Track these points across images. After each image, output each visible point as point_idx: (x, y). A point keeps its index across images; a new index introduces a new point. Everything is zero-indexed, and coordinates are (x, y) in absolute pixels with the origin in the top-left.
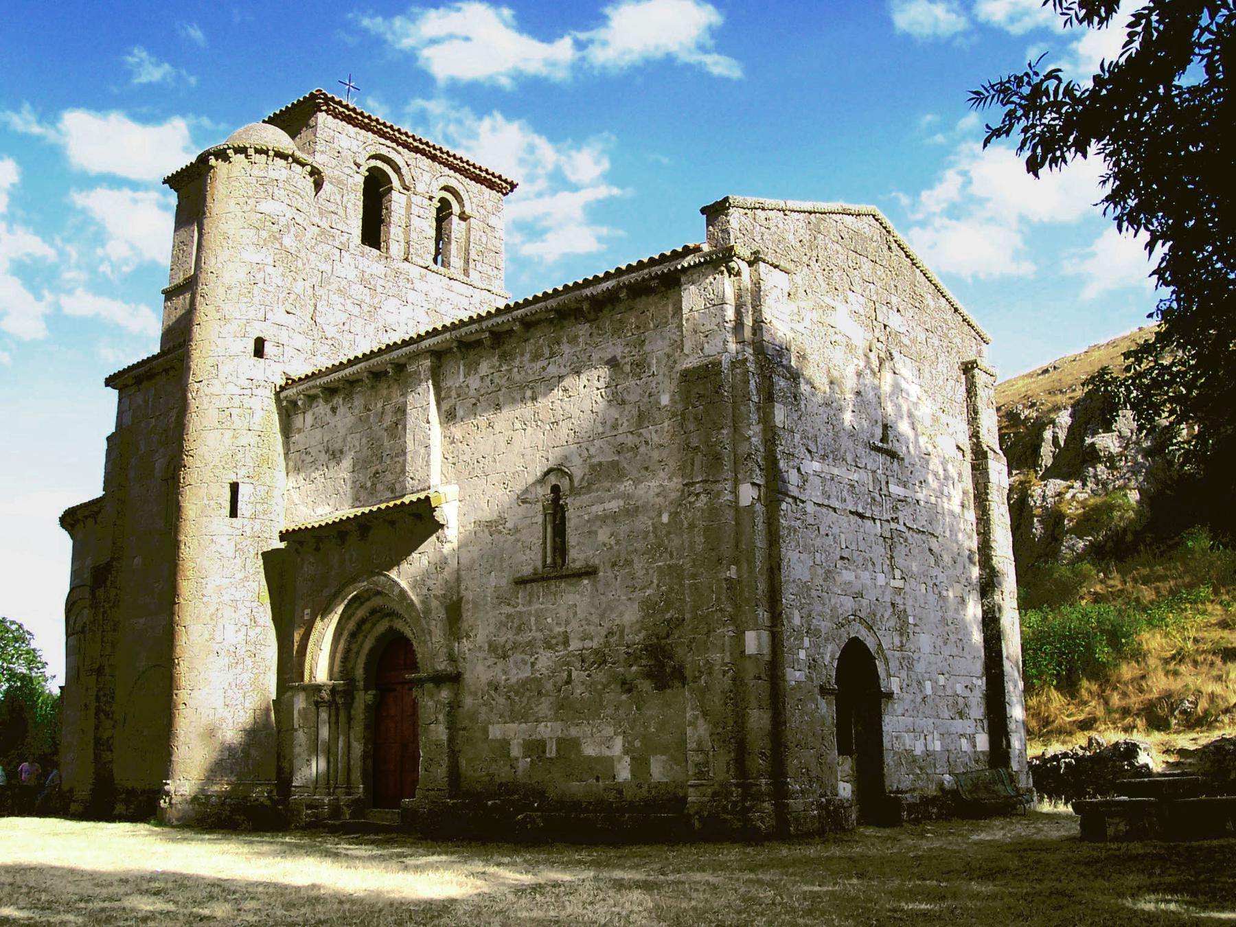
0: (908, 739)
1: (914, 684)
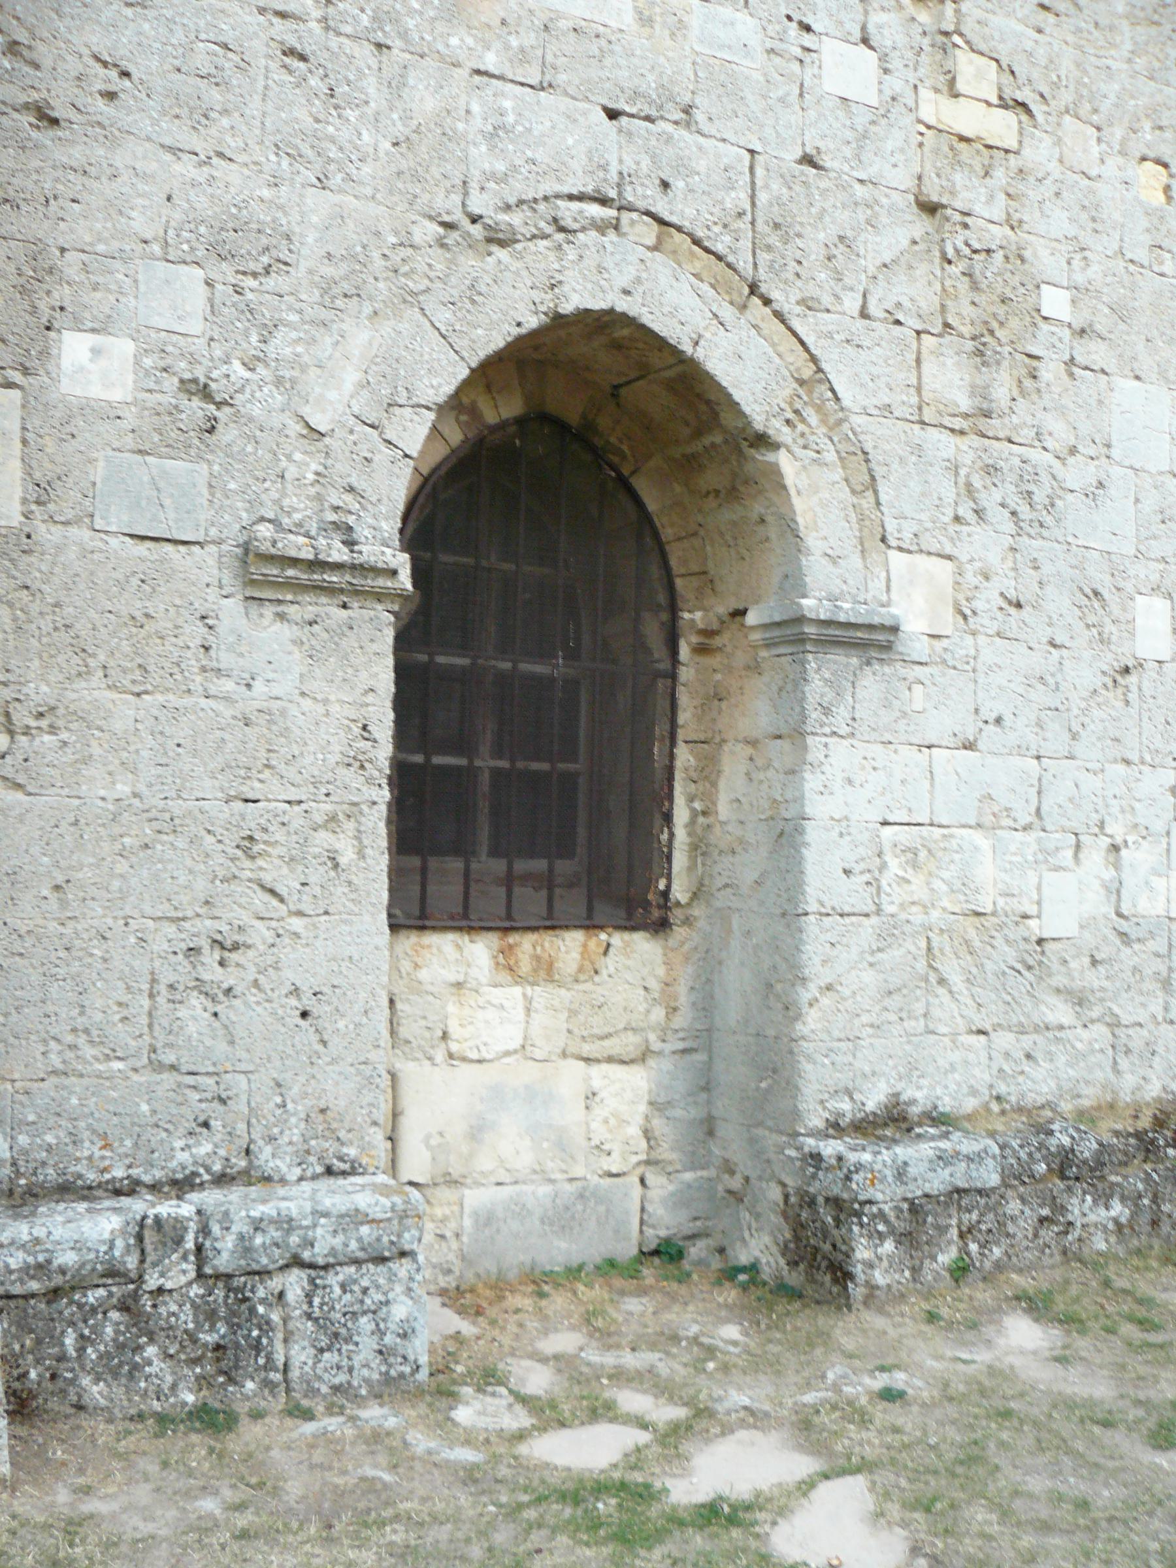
0: (989, 868)
1: (1059, 602)
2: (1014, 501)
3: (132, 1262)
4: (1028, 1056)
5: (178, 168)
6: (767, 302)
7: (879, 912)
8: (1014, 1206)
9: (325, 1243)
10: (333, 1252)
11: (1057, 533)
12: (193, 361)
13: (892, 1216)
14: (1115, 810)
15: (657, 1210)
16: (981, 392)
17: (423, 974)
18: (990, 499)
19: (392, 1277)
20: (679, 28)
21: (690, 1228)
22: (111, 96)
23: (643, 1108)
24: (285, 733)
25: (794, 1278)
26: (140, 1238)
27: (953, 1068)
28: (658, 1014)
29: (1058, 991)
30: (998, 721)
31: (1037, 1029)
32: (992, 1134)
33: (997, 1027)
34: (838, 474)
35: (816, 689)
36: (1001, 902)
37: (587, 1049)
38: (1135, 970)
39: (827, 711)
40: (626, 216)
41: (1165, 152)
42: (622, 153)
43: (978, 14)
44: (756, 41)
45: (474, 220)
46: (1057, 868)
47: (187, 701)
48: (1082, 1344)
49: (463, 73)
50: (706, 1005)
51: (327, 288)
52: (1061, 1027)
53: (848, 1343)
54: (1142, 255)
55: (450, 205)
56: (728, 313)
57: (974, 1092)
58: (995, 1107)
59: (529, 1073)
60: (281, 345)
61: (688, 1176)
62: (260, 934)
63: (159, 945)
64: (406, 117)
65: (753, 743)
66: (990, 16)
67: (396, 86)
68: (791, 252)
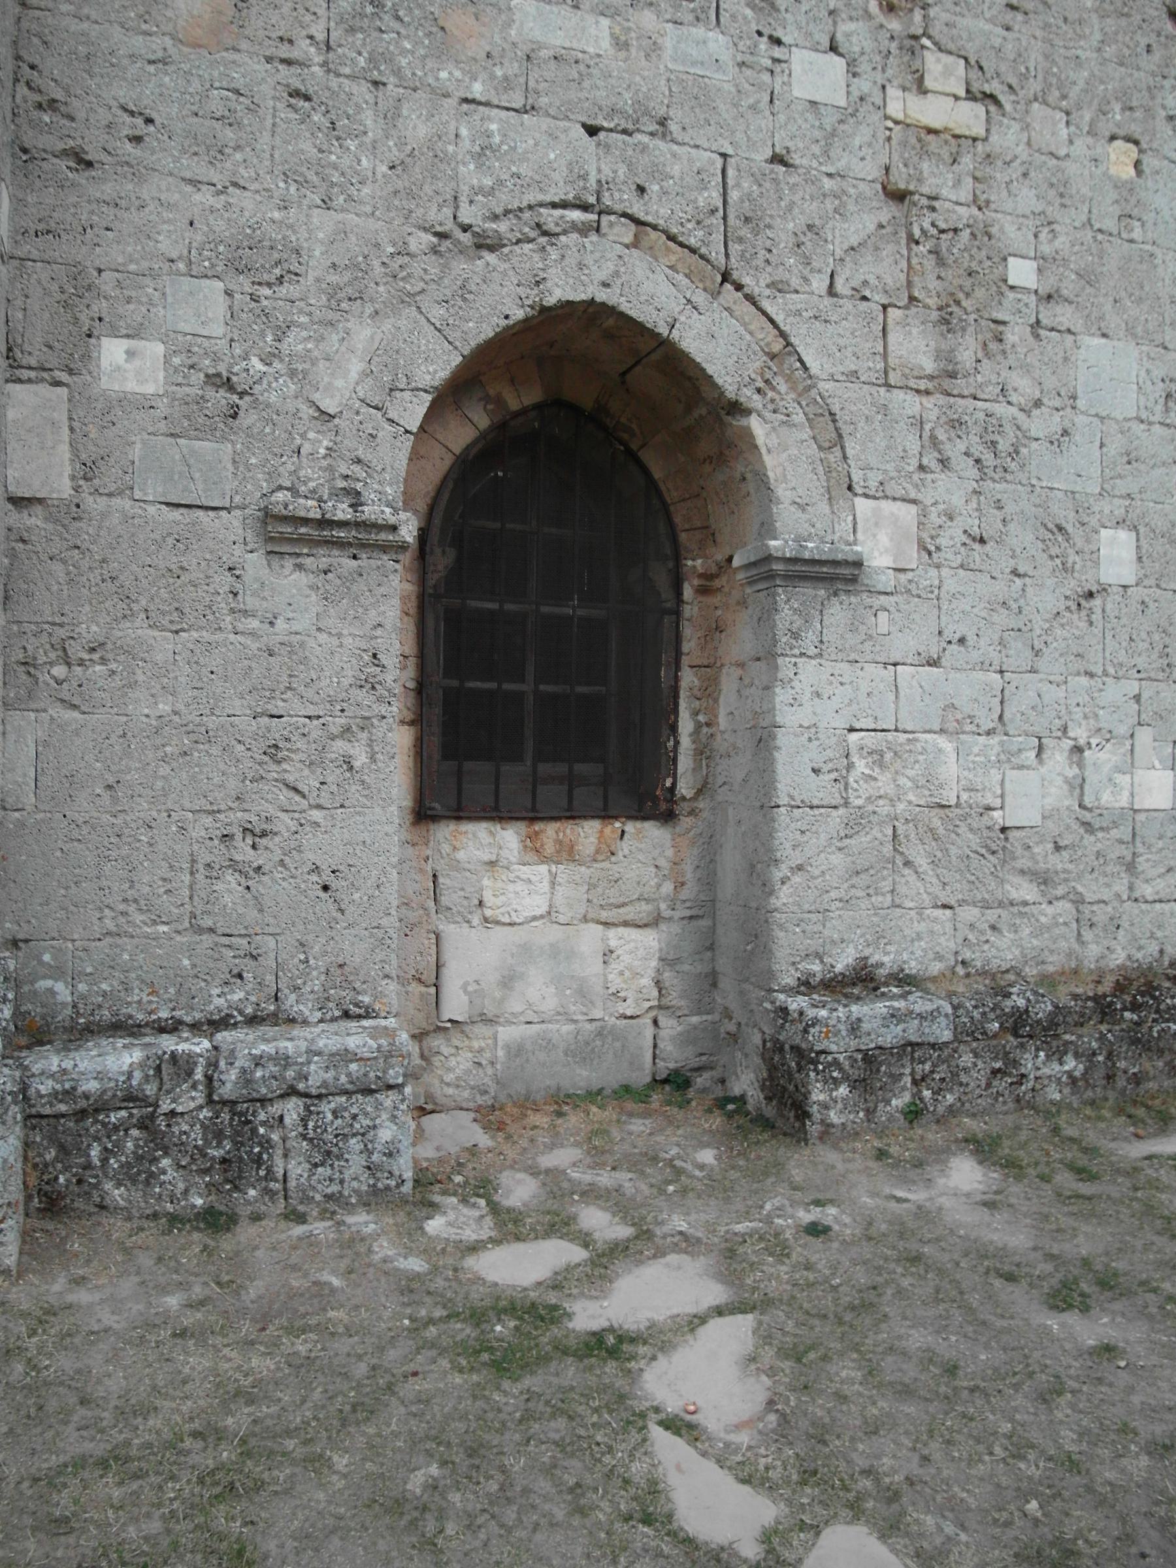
0: (951, 767)
1: (1023, 537)
2: (978, 450)
3: (150, 1090)
4: (993, 928)
5: (198, 197)
6: (739, 287)
7: (846, 804)
8: (967, 1059)
9: (318, 1074)
10: (325, 1084)
11: (1022, 476)
12: (216, 359)
13: (847, 1065)
14: (1078, 716)
15: (666, 1046)
16: (946, 357)
17: (461, 855)
18: (955, 450)
19: (378, 1106)
20: (653, 49)
21: (695, 1062)
22: (137, 139)
23: (654, 963)
24: (304, 661)
25: (770, 1111)
26: (158, 1069)
27: (919, 937)
28: (668, 888)
29: (1022, 872)
30: (962, 641)
31: (1001, 904)
32: (950, 995)
33: (962, 902)
34: (806, 433)
35: (786, 616)
36: (965, 796)
37: (604, 915)
38: (1098, 854)
39: (796, 636)
40: (605, 219)
41: (1136, 130)
42: (599, 164)
43: (945, 17)
44: (726, 56)
45: (465, 228)
46: (1021, 767)
47: (219, 637)
48: (1015, 1189)
49: (452, 102)
50: (709, 880)
51: (333, 292)
52: (1025, 903)
53: (797, 1175)
54: (1110, 224)
55: (442, 217)
56: (700, 298)
57: (939, 957)
58: (960, 970)
59: (554, 934)
60: (294, 342)
61: (695, 1019)
62: (285, 823)
63: (197, 832)
64: (401, 143)
65: (741, 665)
66: (958, 19)
67: (391, 117)
68: (761, 242)
